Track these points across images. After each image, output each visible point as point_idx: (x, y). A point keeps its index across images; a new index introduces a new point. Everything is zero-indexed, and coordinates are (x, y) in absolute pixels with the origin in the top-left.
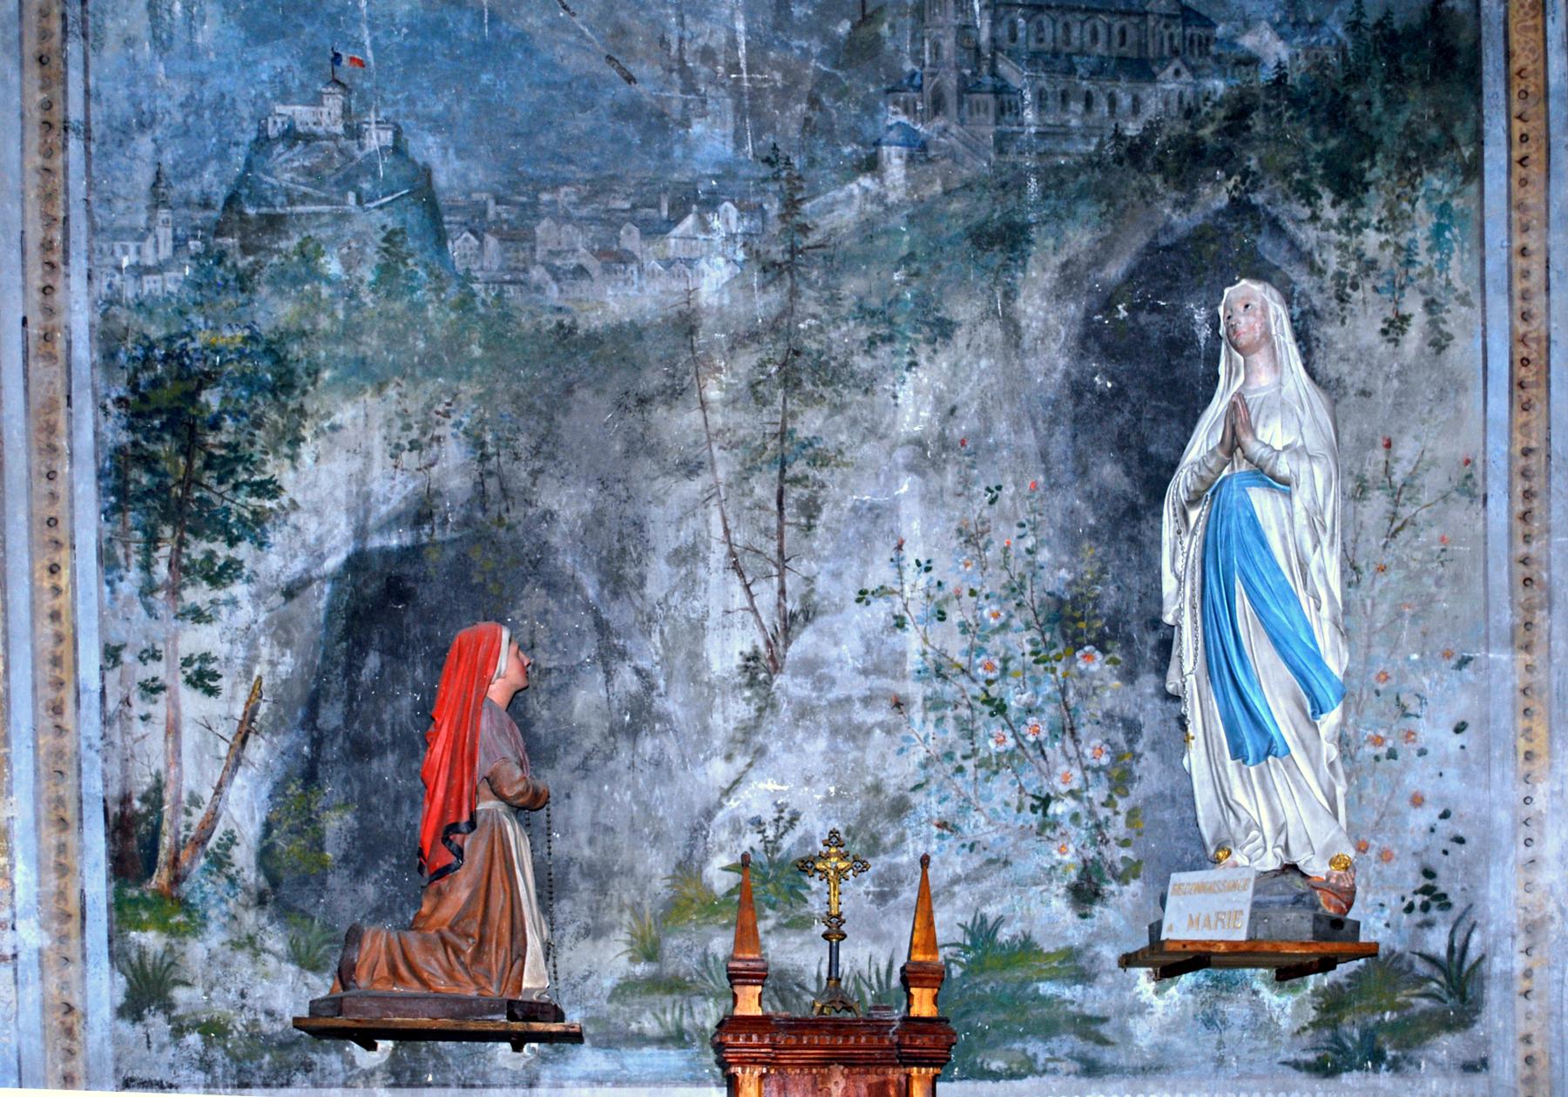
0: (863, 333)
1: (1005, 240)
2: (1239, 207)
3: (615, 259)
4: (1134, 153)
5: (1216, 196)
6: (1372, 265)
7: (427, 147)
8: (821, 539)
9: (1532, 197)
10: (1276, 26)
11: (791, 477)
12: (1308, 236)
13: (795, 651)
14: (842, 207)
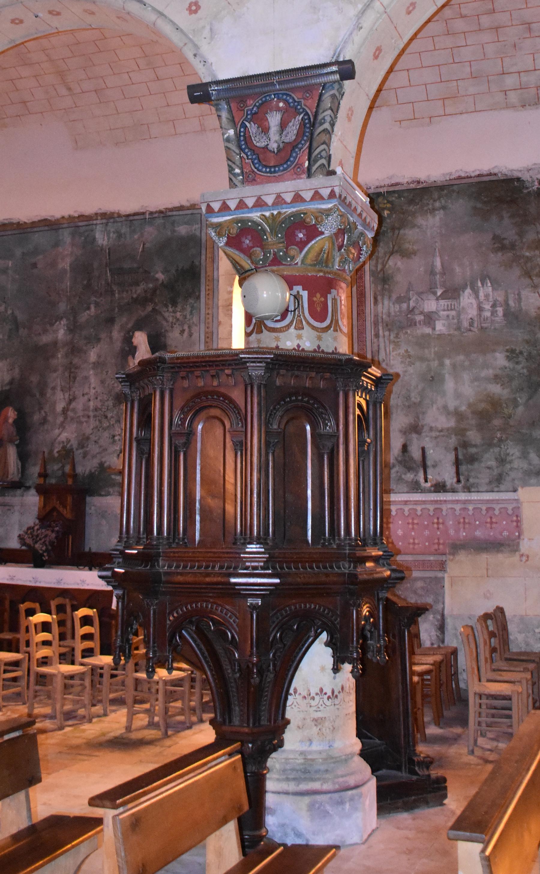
0: (85, 342)
1: (111, 321)
2: (154, 310)
3: (45, 331)
4: (135, 301)
5: (149, 308)
6: (178, 320)
7: (17, 313)
8: (76, 384)
9: (210, 302)
10: (162, 272)
11: (72, 373)
12: (166, 314)
13: (71, 406)
14: (84, 317)
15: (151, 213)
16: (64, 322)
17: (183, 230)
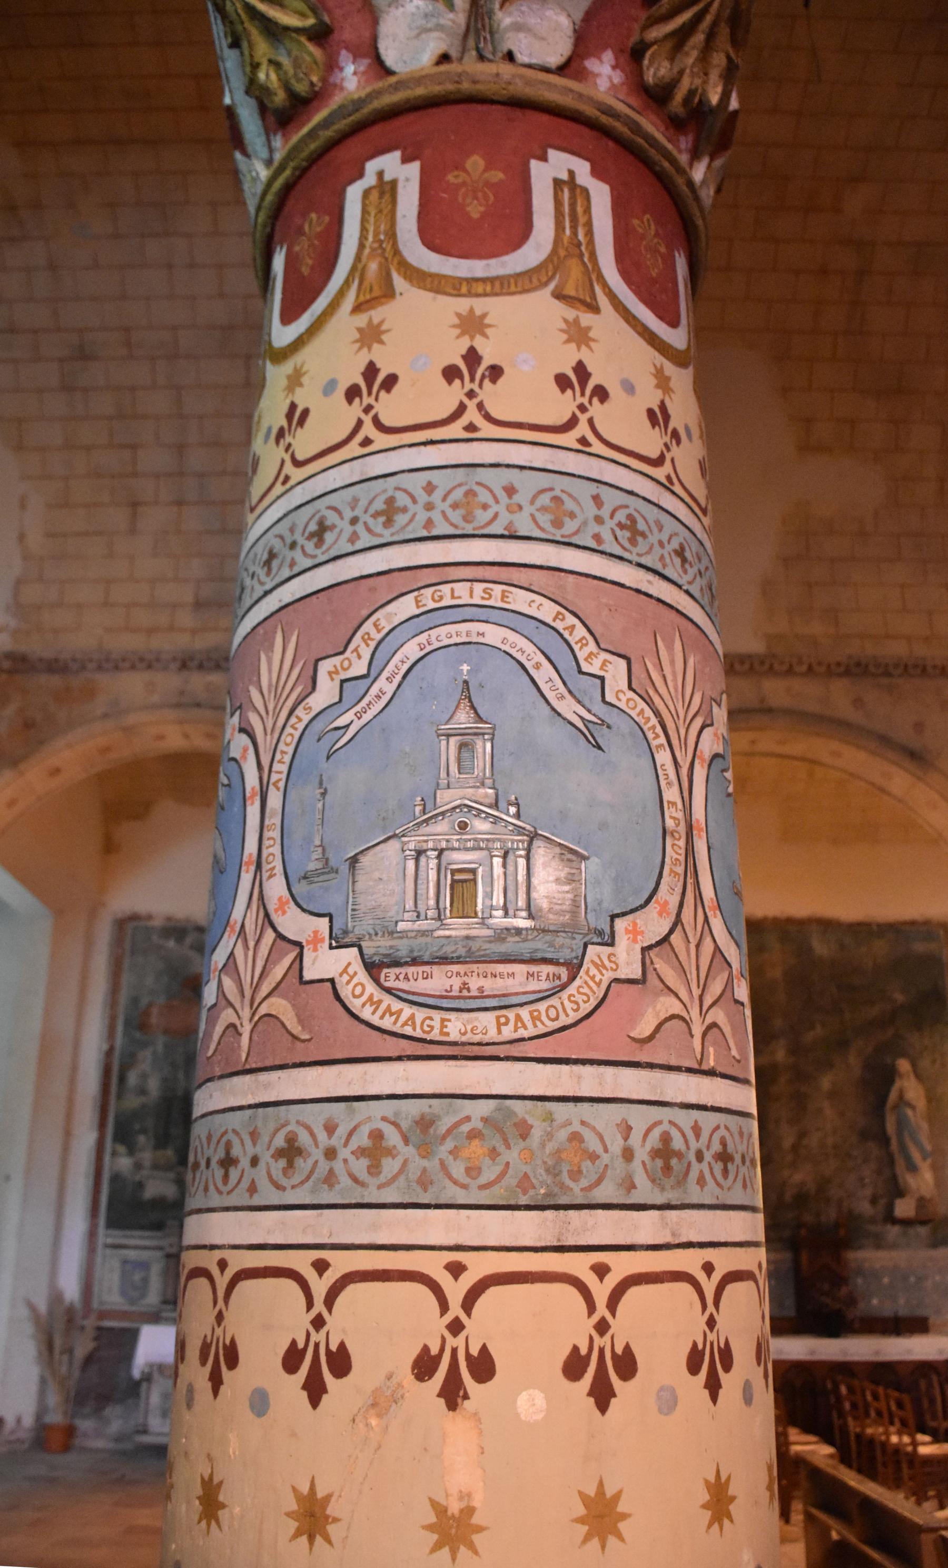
1: (843, 1044)
14: (809, 1037)
15: (879, 925)
16: (782, 1042)
17: (919, 947)
